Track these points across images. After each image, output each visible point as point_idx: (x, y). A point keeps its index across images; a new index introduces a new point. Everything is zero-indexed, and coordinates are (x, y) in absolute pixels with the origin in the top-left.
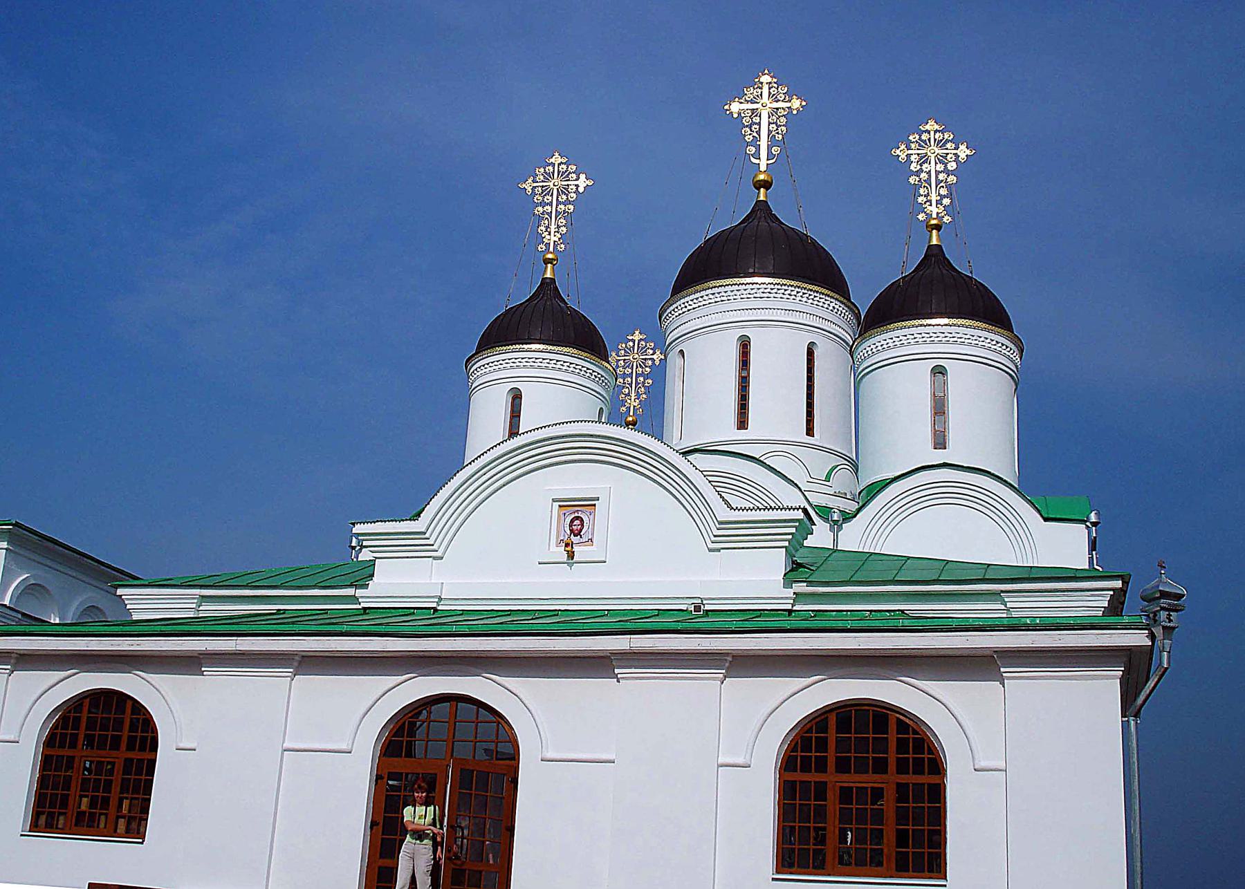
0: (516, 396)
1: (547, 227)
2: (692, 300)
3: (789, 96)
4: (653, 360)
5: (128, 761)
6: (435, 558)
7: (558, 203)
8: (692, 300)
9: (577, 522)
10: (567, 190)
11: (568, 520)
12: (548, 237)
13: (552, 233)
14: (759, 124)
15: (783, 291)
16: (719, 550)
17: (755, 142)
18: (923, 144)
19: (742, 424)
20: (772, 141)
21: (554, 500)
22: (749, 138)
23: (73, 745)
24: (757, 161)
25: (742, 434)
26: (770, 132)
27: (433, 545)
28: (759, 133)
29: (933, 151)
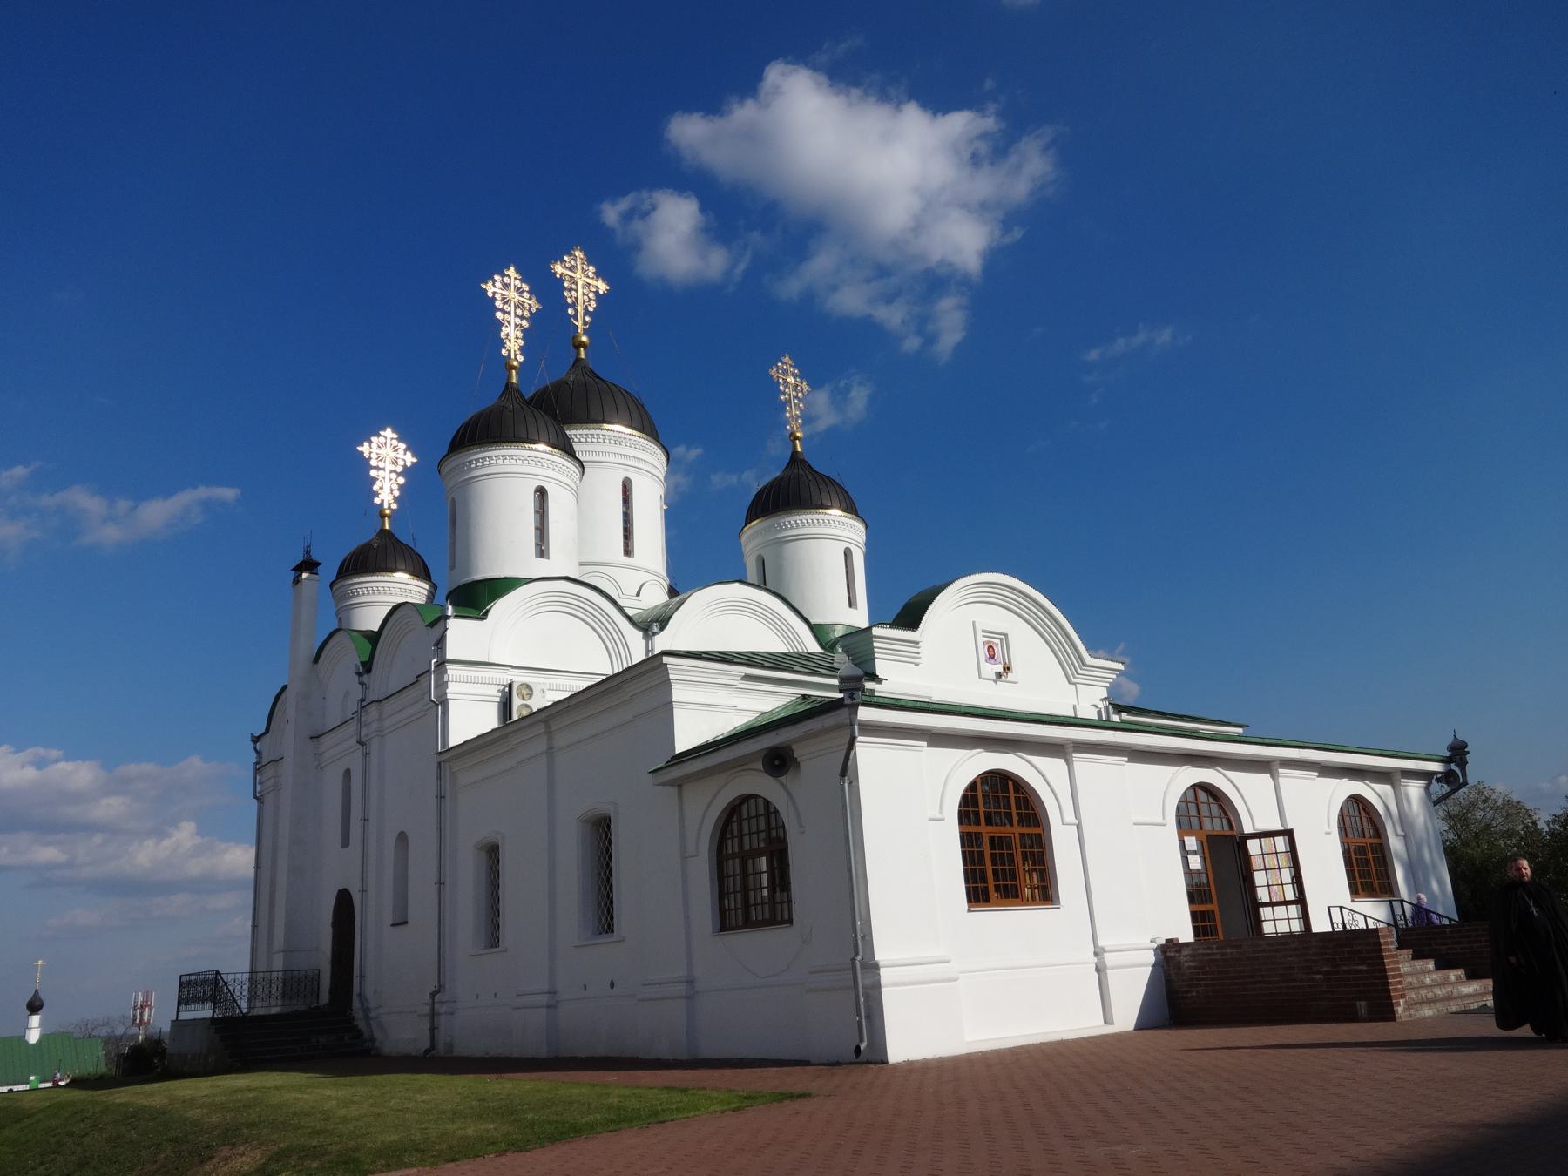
0: (541, 492)
1: (508, 335)
2: (580, 435)
3: (598, 275)
4: (404, 460)
5: (1022, 835)
6: (917, 665)
7: (516, 315)
8: (580, 435)
9: (991, 649)
10: (522, 305)
11: (986, 647)
12: (508, 343)
13: (513, 341)
14: (576, 291)
15: (651, 448)
16: (1075, 684)
17: (574, 305)
18: (785, 372)
19: (628, 551)
20: (586, 312)
21: (984, 631)
22: (569, 301)
23: (978, 823)
24: (576, 323)
25: (627, 560)
26: (584, 302)
27: (918, 653)
28: (576, 298)
29: (791, 379)
